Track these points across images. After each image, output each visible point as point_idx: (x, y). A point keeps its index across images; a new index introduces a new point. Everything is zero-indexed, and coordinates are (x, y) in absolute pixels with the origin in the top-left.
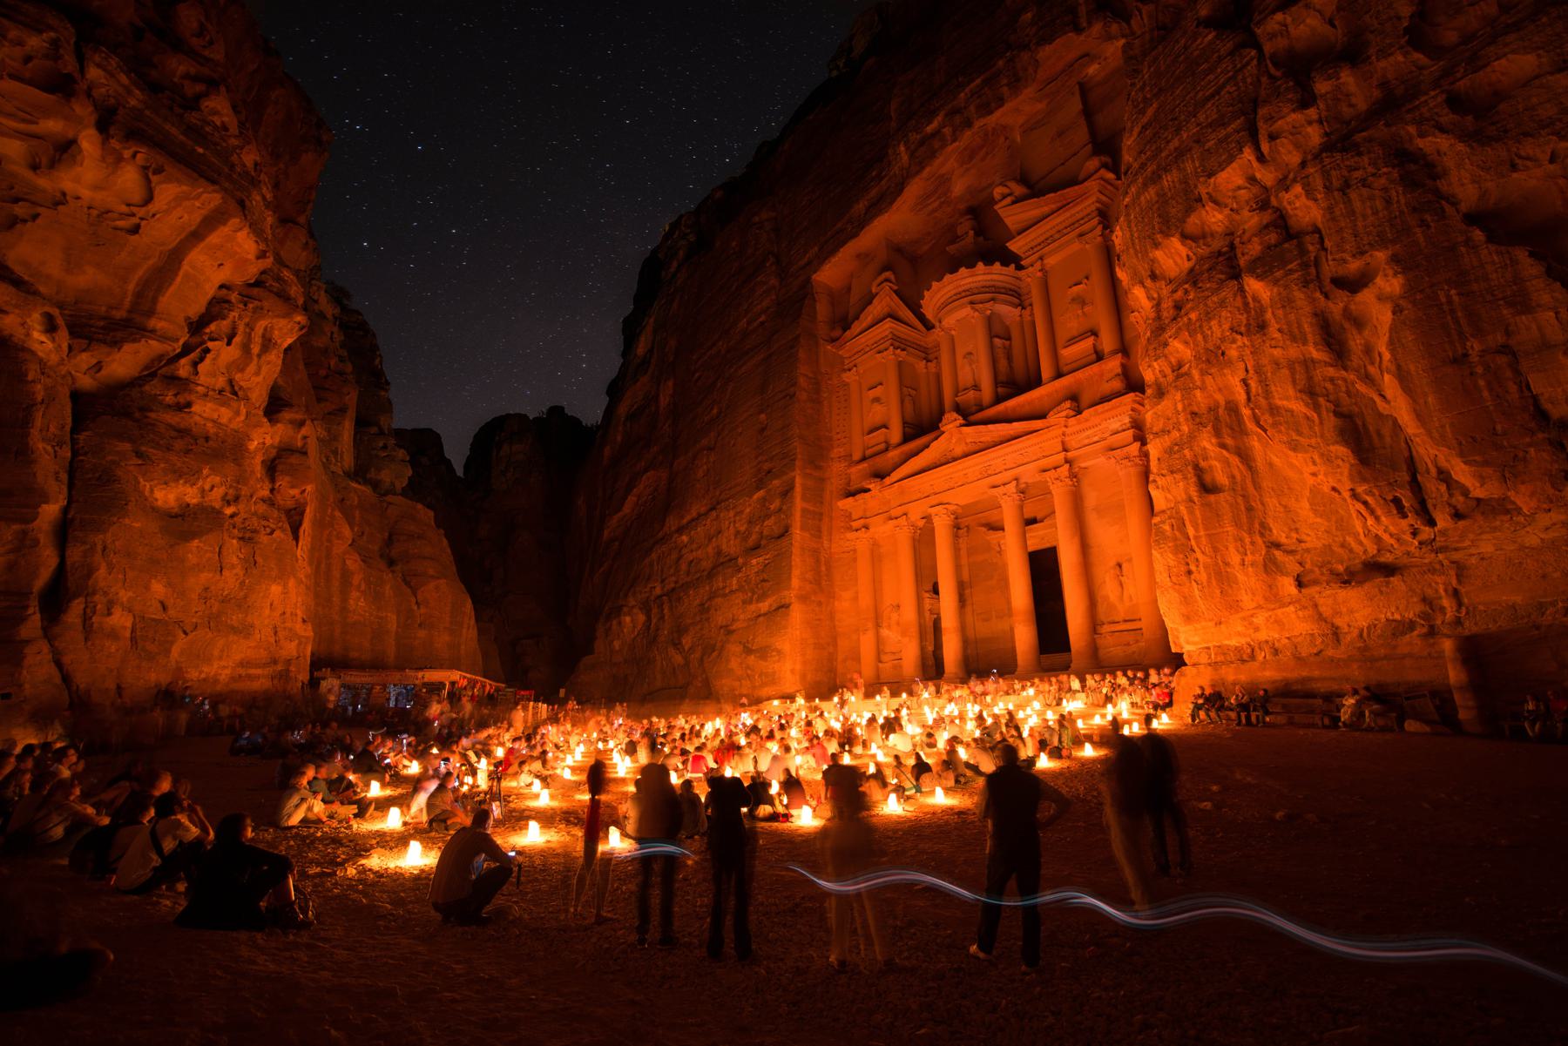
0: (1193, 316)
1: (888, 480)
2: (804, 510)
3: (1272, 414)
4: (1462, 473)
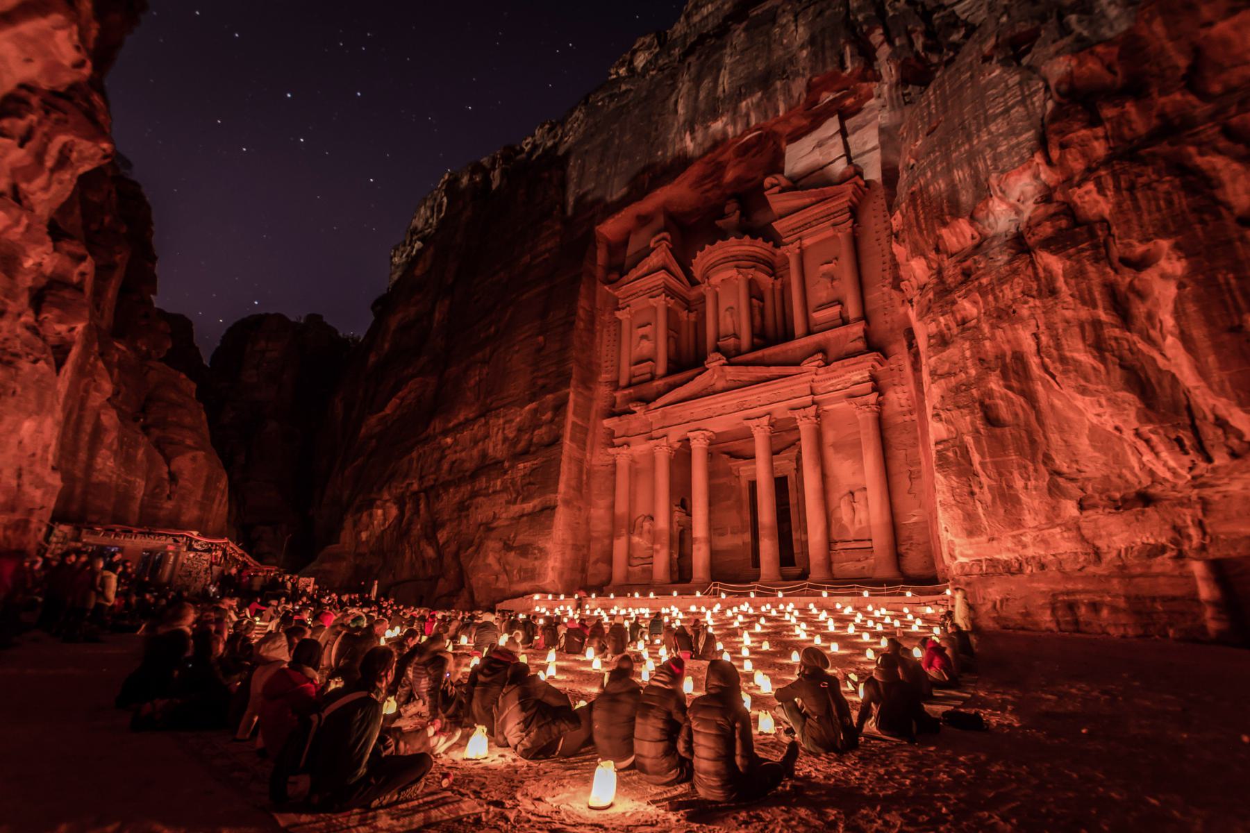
0: (985, 281)
1: (652, 406)
2: (574, 424)
4: (1237, 418)
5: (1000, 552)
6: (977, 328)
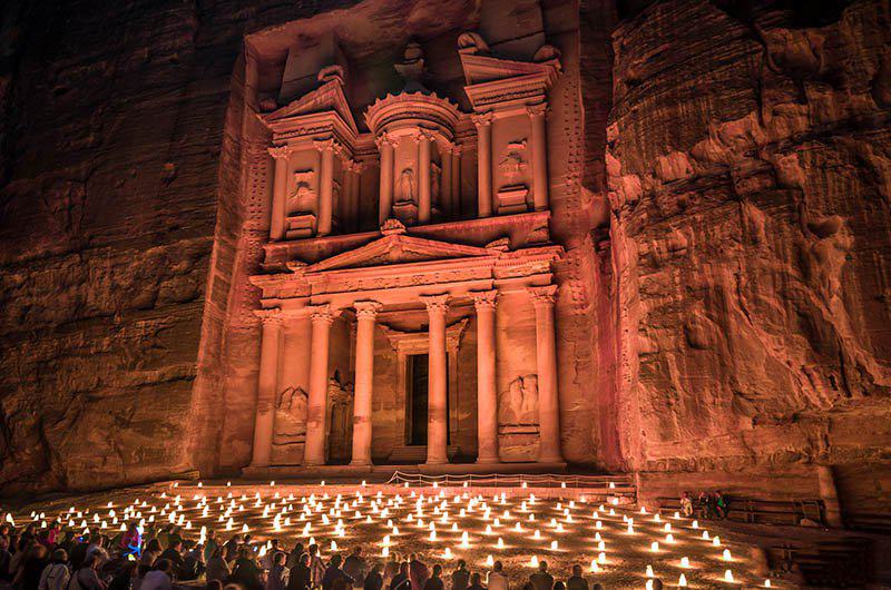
1: (315, 268)
2: (216, 278)
3: (755, 304)
4: (873, 368)
5: (681, 453)
6: (686, 257)
